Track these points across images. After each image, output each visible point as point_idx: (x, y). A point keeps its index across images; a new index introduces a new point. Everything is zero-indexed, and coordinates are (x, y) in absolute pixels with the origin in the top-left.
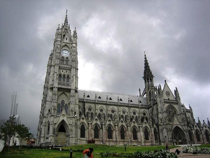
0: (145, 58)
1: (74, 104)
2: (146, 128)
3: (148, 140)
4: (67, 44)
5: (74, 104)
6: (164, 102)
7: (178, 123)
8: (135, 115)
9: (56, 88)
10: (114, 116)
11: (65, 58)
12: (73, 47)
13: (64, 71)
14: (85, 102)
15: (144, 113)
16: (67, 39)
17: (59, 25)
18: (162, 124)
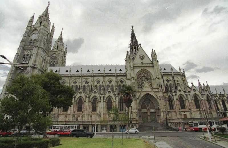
0: (133, 29)
4: (36, 28)
6: (134, 67)
7: (150, 90)
11: (33, 40)
12: (41, 29)
13: (28, 51)
17: (34, 14)
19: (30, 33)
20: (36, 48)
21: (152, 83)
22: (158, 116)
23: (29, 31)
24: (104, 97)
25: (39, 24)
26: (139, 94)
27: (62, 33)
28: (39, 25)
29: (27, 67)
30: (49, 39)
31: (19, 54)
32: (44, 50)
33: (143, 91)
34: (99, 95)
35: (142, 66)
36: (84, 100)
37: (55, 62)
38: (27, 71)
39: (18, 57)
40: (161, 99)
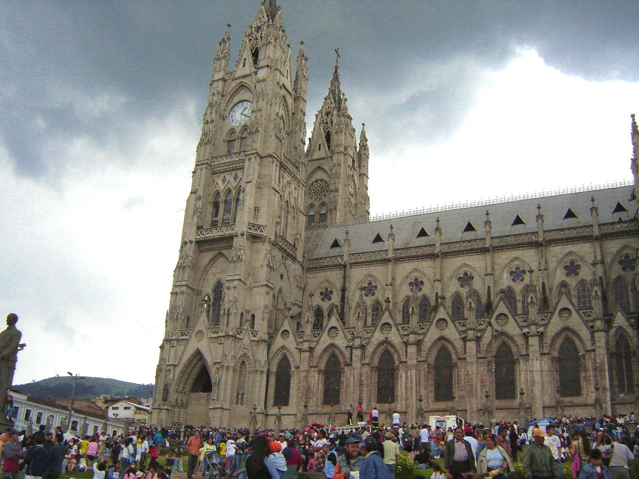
2: (567, 339)
3: (578, 393)
8: (577, 274)
9: (189, 245)
11: (238, 130)
12: (259, 82)
13: (229, 177)
14: (345, 266)
15: (627, 256)
16: (247, 63)
19: (223, 106)
23: (220, 96)
24: (541, 335)
25: (250, 60)
27: (336, 72)
28: (249, 68)
29: (230, 238)
30: (293, 114)
31: (201, 194)
32: (281, 163)
36: (456, 353)
37: (323, 204)
38: (231, 254)
39: (198, 205)
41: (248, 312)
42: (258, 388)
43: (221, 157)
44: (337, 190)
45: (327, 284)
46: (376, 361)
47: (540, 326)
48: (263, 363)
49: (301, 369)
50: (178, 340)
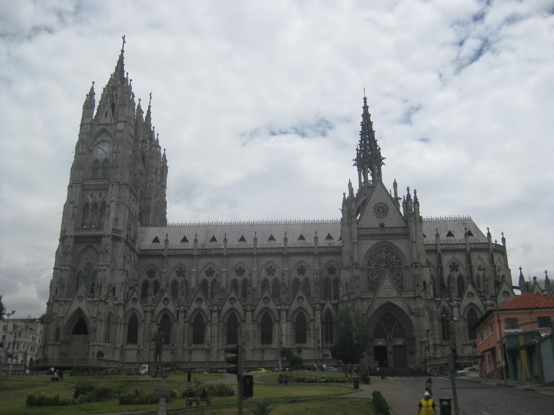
0: (366, 108)
1: (104, 270)
4: (108, 128)
5: (104, 270)
7: (395, 294)
8: (304, 274)
9: (69, 238)
10: (212, 286)
11: (101, 162)
12: (118, 131)
13: (96, 195)
15: (332, 267)
16: (108, 115)
18: (345, 299)
20: (115, 186)
21: (402, 276)
22: (411, 353)
24: (287, 311)
25: (110, 113)
26: (370, 303)
29: (100, 237)
31: (77, 204)
33: (378, 298)
34: (277, 305)
35: (380, 235)
36: (240, 317)
40: (418, 317)
41: (110, 285)
42: (121, 333)
43: (90, 179)
44: (150, 199)
45: (151, 267)
46: (193, 320)
47: (287, 305)
48: (121, 318)
49: (146, 323)
50: (65, 301)
